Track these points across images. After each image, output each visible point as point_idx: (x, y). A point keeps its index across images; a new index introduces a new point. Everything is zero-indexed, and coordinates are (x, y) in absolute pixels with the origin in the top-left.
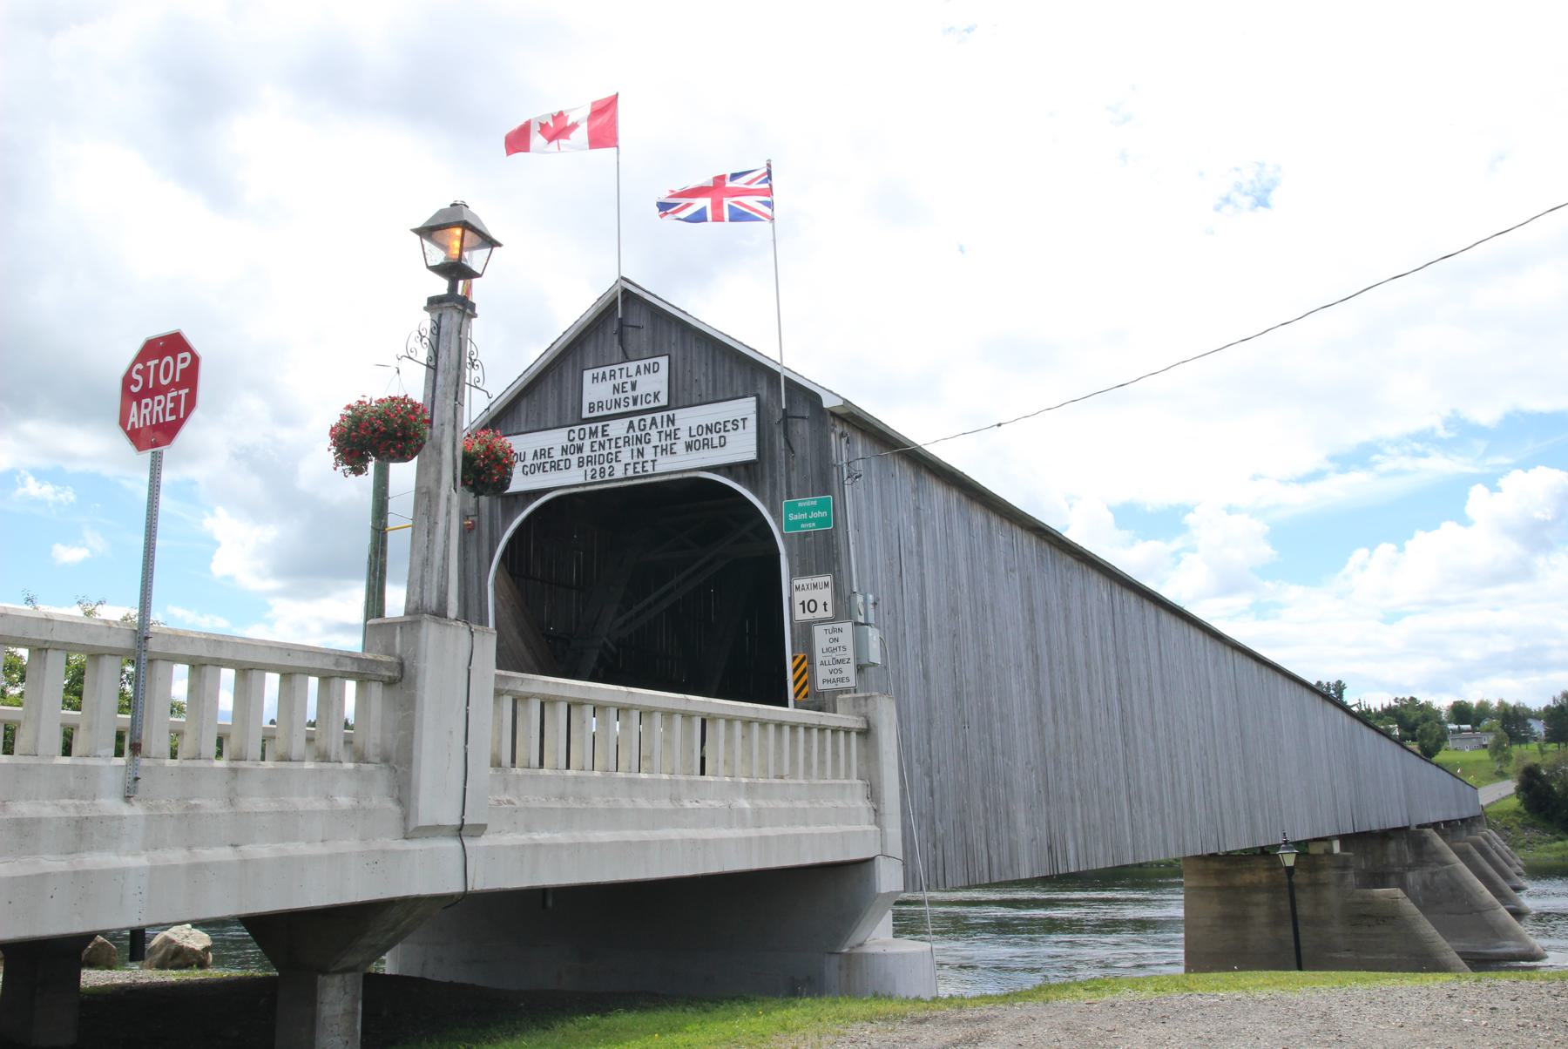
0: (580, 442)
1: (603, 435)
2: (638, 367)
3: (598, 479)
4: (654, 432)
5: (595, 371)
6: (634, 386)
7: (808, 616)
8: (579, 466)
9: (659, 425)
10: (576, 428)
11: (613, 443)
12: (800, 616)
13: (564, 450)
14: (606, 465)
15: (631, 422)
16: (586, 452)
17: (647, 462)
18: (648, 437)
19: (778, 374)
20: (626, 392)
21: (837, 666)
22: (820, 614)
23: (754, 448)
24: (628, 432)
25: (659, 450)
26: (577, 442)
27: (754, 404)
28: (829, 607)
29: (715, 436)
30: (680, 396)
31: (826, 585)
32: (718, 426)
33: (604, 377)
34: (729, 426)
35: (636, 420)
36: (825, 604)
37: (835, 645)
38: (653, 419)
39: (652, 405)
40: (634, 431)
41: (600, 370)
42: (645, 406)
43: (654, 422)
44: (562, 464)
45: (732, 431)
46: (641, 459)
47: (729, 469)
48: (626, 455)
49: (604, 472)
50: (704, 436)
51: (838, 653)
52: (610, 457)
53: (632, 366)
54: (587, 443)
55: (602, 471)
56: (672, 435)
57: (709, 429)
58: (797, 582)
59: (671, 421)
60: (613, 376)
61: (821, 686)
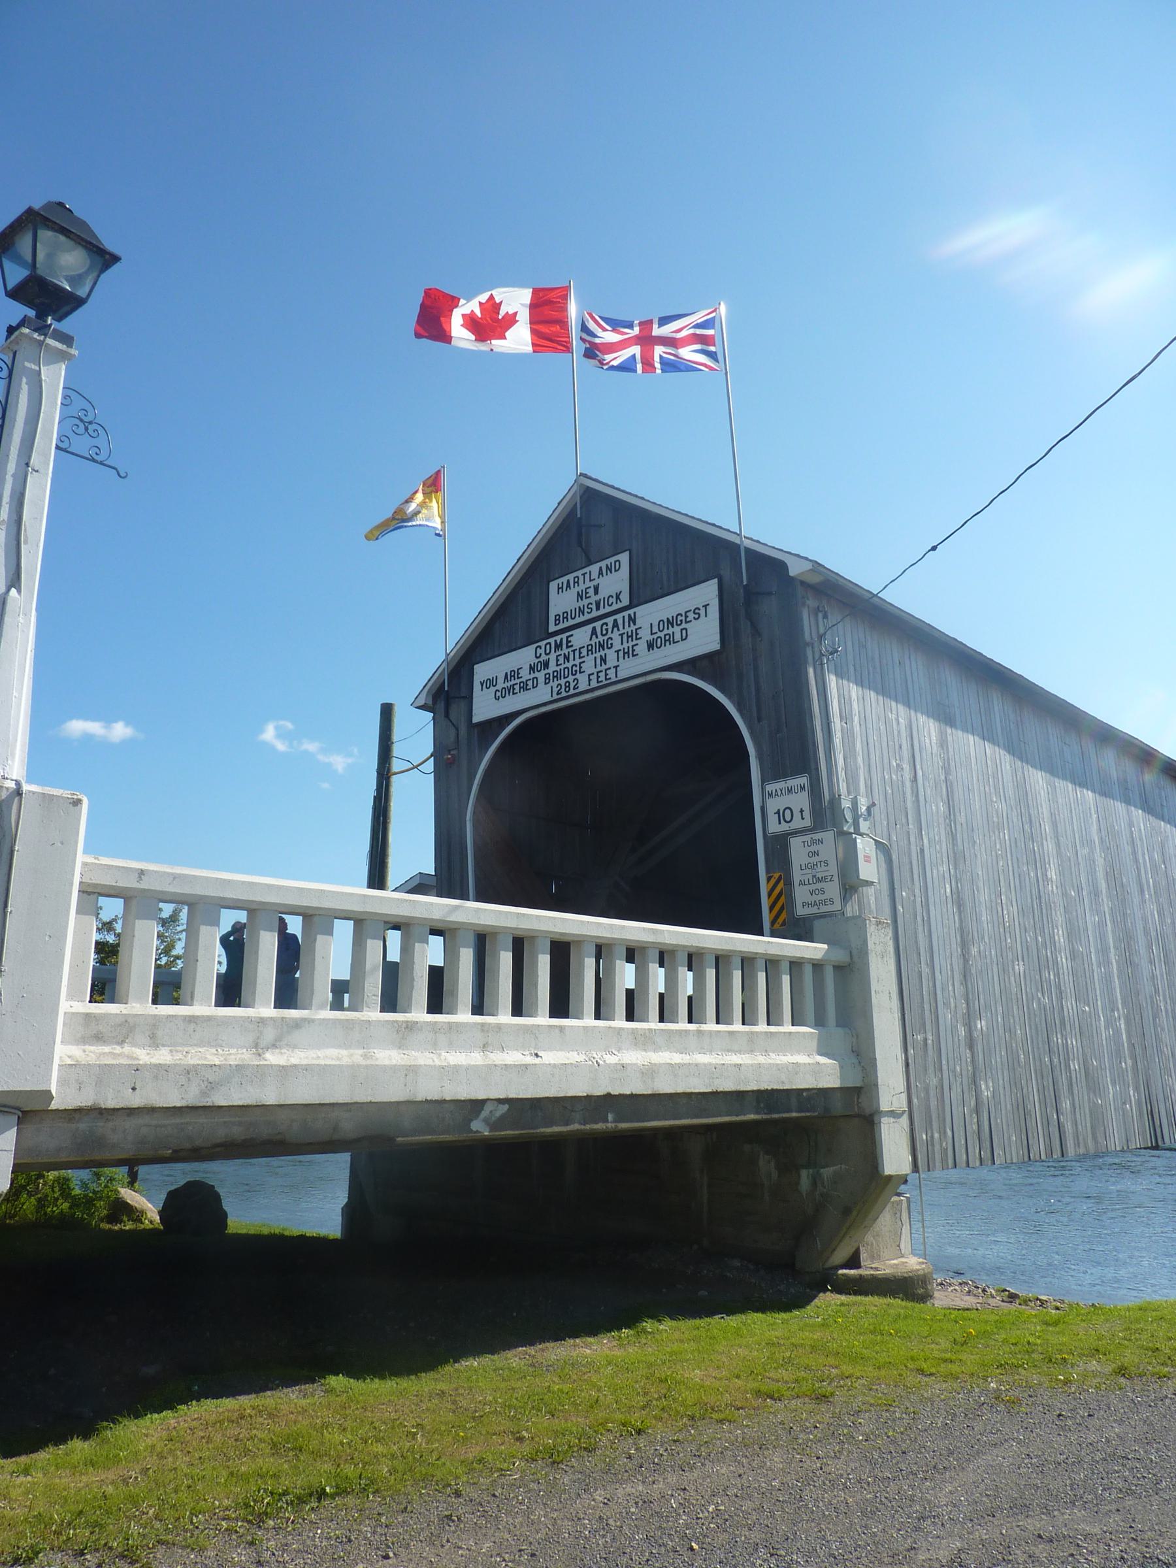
1: (568, 647)
3: (564, 694)
4: (615, 636)
5: (560, 581)
6: (596, 592)
7: (784, 827)
8: (546, 683)
9: (621, 627)
10: (542, 644)
11: (577, 653)
12: (774, 827)
15: (594, 629)
16: (552, 667)
17: (610, 668)
18: (610, 642)
19: (737, 547)
20: (590, 597)
21: (819, 886)
22: (797, 823)
23: (717, 637)
24: (591, 639)
25: (621, 654)
26: (544, 658)
27: (716, 587)
28: (807, 814)
29: (677, 629)
31: (802, 788)
33: (568, 586)
34: (691, 616)
35: (598, 625)
36: (802, 811)
37: (815, 860)
38: (615, 621)
39: (615, 607)
40: (597, 637)
41: (564, 579)
42: (608, 609)
44: (530, 683)
45: (693, 620)
47: (690, 665)
48: (589, 666)
49: (569, 686)
50: (666, 631)
51: (819, 869)
52: (574, 668)
53: (594, 569)
54: (553, 657)
56: (634, 636)
57: (670, 623)
58: (770, 788)
59: (632, 620)
60: (576, 582)
61: (801, 911)
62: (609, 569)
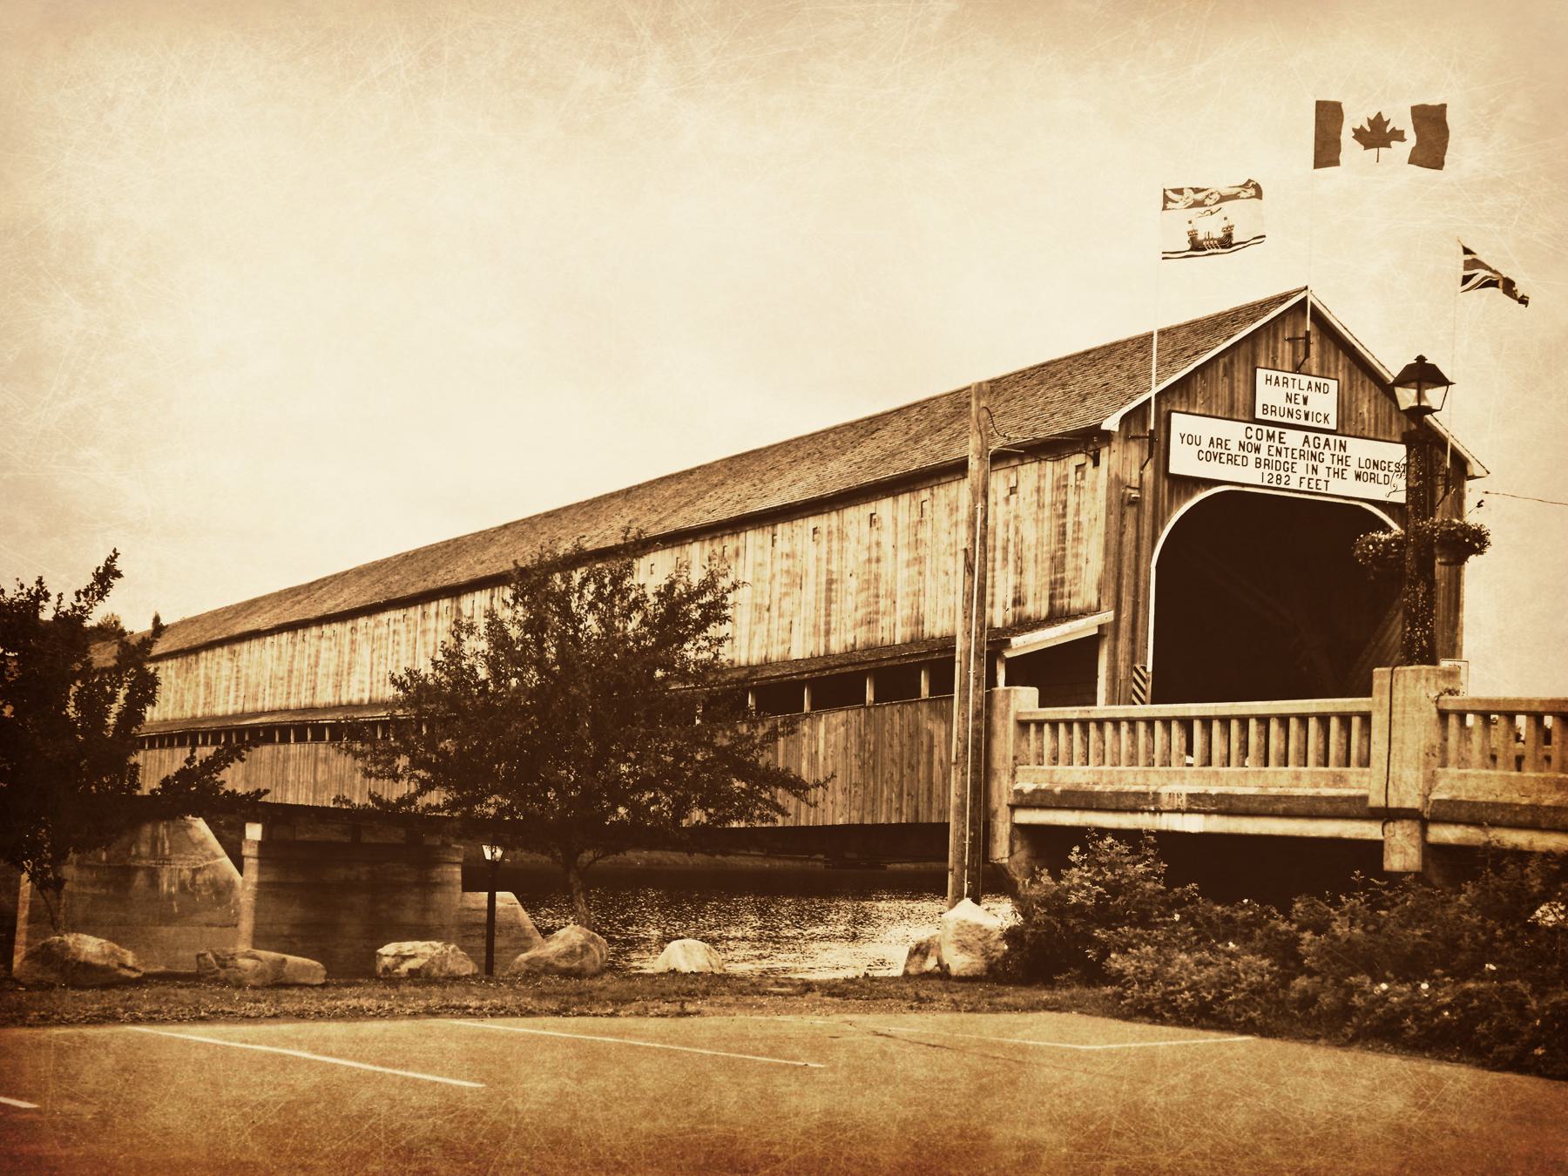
0: (1258, 443)
2: (1310, 383)
3: (1274, 485)
5: (1270, 373)
6: (1305, 401)
10: (1255, 427)
11: (1289, 452)
13: (1242, 446)
14: (1283, 473)
16: (1263, 454)
25: (1331, 471)
26: (1254, 440)
29: (1382, 474)
30: (1347, 424)
32: (1383, 465)
35: (1311, 435)
41: (1274, 374)
42: (1315, 424)
43: (1327, 443)
46: (1315, 477)
48: (1301, 466)
53: (1305, 380)
55: (1279, 478)
57: (1376, 465)
59: (1343, 446)
62: (1318, 387)
